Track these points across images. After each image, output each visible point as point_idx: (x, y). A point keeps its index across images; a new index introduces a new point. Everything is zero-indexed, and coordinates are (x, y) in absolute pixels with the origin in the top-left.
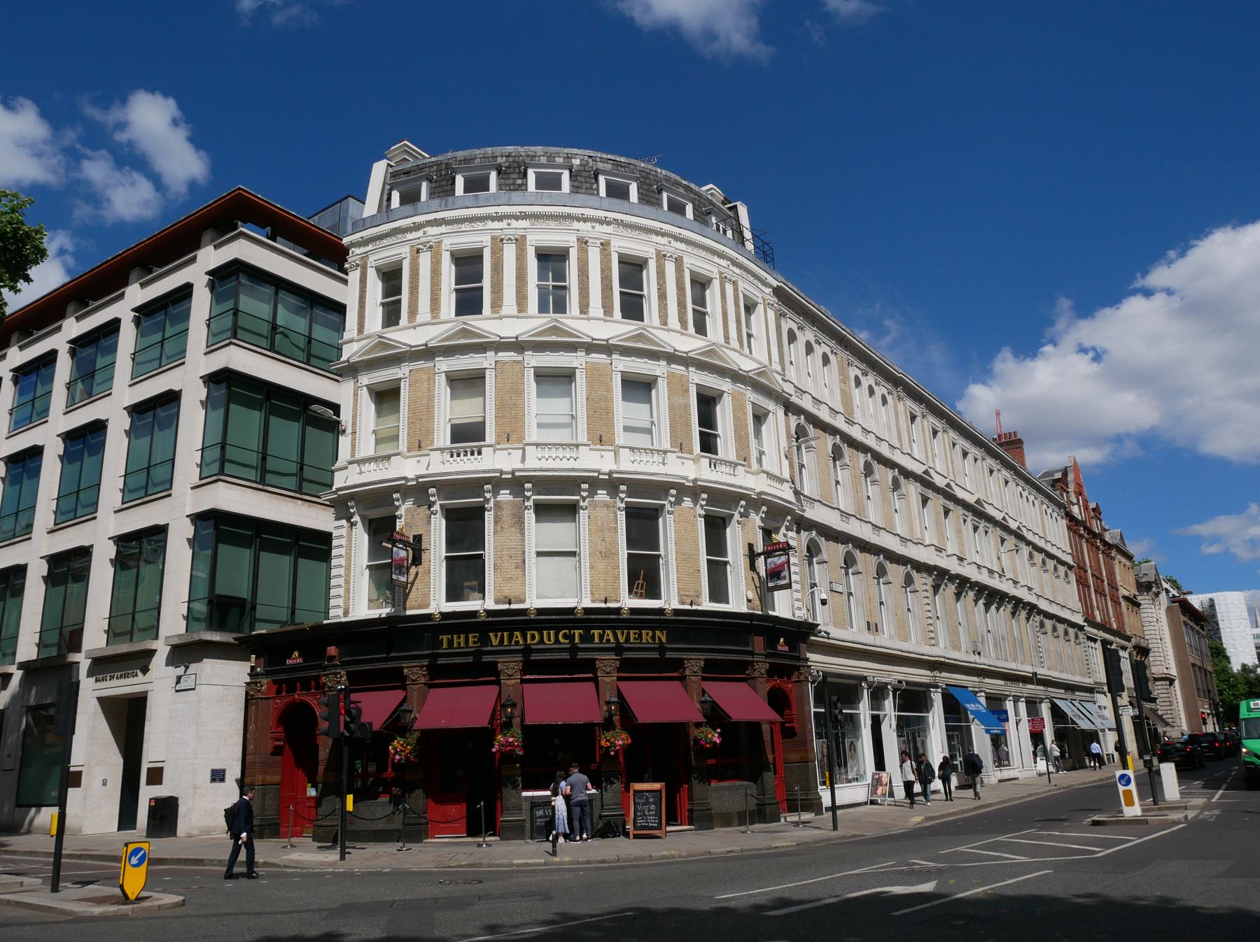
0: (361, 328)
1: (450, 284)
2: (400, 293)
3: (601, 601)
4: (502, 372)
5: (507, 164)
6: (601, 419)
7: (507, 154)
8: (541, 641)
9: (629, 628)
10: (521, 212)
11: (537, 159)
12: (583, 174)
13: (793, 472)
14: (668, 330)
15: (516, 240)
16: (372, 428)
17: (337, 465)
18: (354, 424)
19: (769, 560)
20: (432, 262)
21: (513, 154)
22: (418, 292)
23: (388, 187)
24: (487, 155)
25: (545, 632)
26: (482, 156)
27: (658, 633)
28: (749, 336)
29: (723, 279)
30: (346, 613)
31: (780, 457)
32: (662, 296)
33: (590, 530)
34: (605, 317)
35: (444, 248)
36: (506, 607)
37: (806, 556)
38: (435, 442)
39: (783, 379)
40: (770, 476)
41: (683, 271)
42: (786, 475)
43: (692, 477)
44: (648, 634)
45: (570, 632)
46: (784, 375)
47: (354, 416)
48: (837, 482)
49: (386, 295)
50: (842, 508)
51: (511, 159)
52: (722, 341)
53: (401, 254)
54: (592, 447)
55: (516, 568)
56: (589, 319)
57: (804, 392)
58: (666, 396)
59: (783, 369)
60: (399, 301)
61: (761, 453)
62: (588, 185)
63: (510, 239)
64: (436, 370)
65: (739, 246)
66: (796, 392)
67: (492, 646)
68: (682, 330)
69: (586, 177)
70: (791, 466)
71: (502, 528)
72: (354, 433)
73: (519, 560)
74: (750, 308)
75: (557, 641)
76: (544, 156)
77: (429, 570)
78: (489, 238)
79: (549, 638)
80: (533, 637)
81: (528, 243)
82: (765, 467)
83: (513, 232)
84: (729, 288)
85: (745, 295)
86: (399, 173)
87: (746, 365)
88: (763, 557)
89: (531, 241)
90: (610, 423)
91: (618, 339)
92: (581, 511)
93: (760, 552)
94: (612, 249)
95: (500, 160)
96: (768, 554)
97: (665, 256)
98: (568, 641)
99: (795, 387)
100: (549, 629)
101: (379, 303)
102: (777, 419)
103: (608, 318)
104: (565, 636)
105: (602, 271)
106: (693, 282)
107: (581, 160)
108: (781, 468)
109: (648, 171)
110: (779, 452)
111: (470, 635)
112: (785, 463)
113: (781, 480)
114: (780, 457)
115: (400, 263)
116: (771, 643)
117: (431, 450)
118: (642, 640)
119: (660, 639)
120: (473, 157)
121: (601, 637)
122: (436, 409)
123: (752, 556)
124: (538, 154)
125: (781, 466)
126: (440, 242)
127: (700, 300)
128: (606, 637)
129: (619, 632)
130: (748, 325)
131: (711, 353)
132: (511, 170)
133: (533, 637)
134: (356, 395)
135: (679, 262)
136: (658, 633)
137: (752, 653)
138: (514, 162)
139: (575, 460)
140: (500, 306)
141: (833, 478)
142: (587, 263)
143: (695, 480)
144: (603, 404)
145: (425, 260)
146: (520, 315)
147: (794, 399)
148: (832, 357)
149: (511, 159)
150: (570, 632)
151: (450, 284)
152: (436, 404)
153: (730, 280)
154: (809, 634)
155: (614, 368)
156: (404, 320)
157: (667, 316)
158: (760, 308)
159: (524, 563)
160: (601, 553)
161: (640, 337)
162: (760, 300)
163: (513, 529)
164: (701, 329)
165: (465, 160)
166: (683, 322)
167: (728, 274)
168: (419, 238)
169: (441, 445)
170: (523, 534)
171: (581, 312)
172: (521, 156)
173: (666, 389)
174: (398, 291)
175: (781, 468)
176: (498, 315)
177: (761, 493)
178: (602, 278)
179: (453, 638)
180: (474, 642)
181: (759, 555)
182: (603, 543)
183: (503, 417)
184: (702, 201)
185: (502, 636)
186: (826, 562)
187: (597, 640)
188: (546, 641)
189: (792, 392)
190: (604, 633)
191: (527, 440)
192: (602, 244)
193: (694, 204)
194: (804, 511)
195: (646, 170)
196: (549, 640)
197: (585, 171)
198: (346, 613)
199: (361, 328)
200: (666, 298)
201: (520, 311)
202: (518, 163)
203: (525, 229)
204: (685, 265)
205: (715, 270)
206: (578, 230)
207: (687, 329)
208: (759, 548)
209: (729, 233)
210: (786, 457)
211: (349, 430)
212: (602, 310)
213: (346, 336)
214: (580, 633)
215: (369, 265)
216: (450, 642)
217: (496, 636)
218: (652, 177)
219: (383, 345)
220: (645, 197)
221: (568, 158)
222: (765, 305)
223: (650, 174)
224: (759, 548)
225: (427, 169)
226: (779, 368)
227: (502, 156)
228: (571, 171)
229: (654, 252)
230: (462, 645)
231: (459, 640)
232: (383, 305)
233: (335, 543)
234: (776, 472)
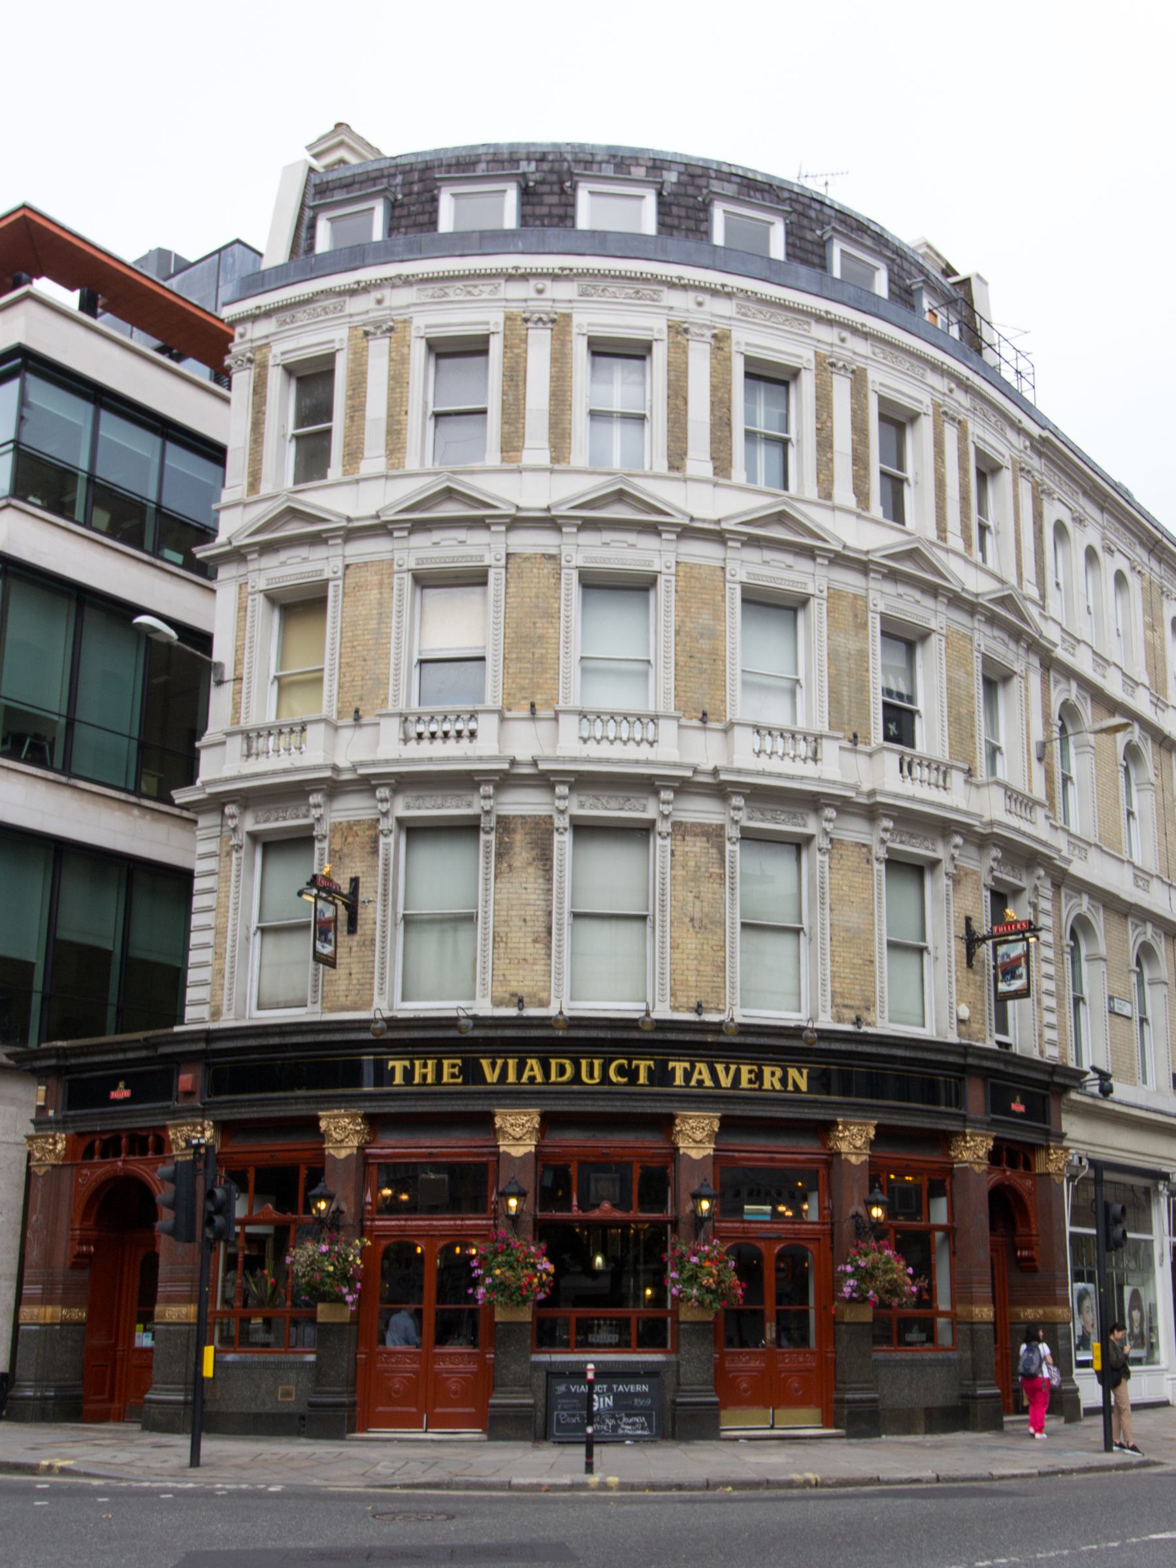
0: (254, 484)
1: (425, 403)
2: (330, 419)
3: (689, 1009)
4: (520, 576)
5: (538, 176)
6: (702, 672)
7: (538, 156)
8: (576, 1080)
9: (740, 1060)
10: (563, 269)
11: (595, 167)
12: (683, 201)
13: (1053, 790)
14: (834, 508)
15: (553, 321)
16: (273, 672)
17: (206, 739)
18: (238, 663)
19: (1002, 950)
20: (391, 360)
21: (550, 157)
22: (363, 417)
23: (308, 213)
24: (500, 157)
25: (584, 1062)
26: (490, 158)
28: (983, 528)
29: (942, 415)
30: (216, 1014)
31: (1029, 759)
32: (825, 443)
33: (673, 877)
34: (716, 479)
35: (414, 333)
36: (512, 1012)
37: (1068, 945)
38: (390, 702)
39: (1041, 614)
40: (1010, 793)
41: (866, 396)
42: (1039, 793)
43: (866, 787)
45: (630, 1064)
46: (1043, 608)
47: (239, 649)
48: (1130, 814)
49: (301, 421)
50: (1138, 861)
51: (546, 166)
52: (932, 535)
53: (332, 341)
54: (684, 722)
55: (535, 941)
56: (685, 480)
57: (1078, 641)
58: (825, 634)
59: (1043, 596)
60: (328, 432)
61: (994, 751)
62: (692, 224)
63: (540, 319)
64: (396, 568)
65: (974, 356)
66: (1063, 640)
67: (483, 1080)
68: (859, 511)
69: (687, 208)
70: (1049, 779)
71: (510, 866)
72: (238, 679)
73: (540, 927)
74: (987, 471)
75: (605, 1079)
76: (608, 162)
77: (373, 940)
78: (500, 318)
79: (591, 1072)
80: (562, 1071)
81: (575, 330)
82: (1002, 774)
83: (546, 306)
84: (951, 434)
85: (978, 450)
86: (331, 186)
87: (975, 583)
88: (990, 942)
89: (580, 326)
90: (717, 681)
91: (738, 520)
92: (659, 841)
93: (985, 933)
94: (734, 348)
95: (524, 167)
96: (999, 940)
97: (832, 365)
98: (625, 1080)
99: (1063, 630)
100: (591, 1055)
101: (289, 436)
102: (1026, 689)
103: (721, 481)
104: (621, 1071)
105: (714, 389)
106: (883, 418)
107: (680, 173)
108: (1030, 781)
109: (807, 201)
110: (1028, 750)
111: (446, 1063)
112: (1038, 772)
113: (1027, 803)
114: (1029, 759)
115: (330, 358)
116: (998, 1102)
117: (381, 716)
118: (762, 1084)
119: (795, 1084)
120: (473, 158)
121: (688, 1075)
122: (393, 640)
123: (972, 941)
124: (598, 158)
125: (1030, 777)
126: (407, 322)
127: (896, 454)
128: (696, 1076)
129: (720, 1068)
130: (982, 510)
131: (913, 555)
132: (545, 189)
133: (562, 1071)
134: (242, 609)
135: (858, 379)
136: (793, 1073)
137: (964, 1119)
138: (551, 171)
139: (651, 744)
140: (518, 449)
141: (1123, 807)
142: (685, 373)
143: (872, 793)
144: (705, 644)
145: (378, 356)
146: (557, 467)
147: (1060, 653)
148: (1131, 578)
149: (546, 166)
150: (630, 1064)
151: (425, 403)
152: (394, 630)
153: (953, 419)
154: (1066, 1089)
155: (728, 577)
156: (335, 472)
157: (831, 482)
158: (1006, 476)
159: (550, 933)
160: (692, 920)
161: (781, 518)
162: (1006, 462)
163: (531, 870)
164: (896, 512)
165: (458, 164)
166: (862, 496)
167: (950, 405)
168: (367, 312)
169: (402, 707)
170: (549, 880)
171: (672, 467)
172: (565, 160)
173: (825, 620)
174: (326, 413)
175: (1030, 781)
176: (513, 466)
177: (992, 823)
178: (712, 403)
179: (413, 1065)
180: (453, 1076)
181: (984, 939)
182: (697, 903)
183: (519, 659)
184: (906, 265)
186: (1104, 960)
188: (584, 1077)
189: (1058, 640)
190: (693, 1067)
191: (561, 705)
192: (715, 336)
193: (890, 271)
194: (1069, 862)
195: (801, 199)
196: (591, 1076)
197: (687, 195)
198: (216, 1014)
199: (254, 484)
200: (831, 447)
201: (555, 460)
202: (559, 173)
203: (570, 301)
204: (870, 386)
205: (927, 400)
206: (671, 308)
207: (867, 508)
208: (983, 925)
209: (954, 332)
210: (1040, 759)
211: (228, 674)
213: (227, 496)
214: (649, 1068)
215: (271, 362)
216: (408, 1074)
217: (493, 1065)
218: (813, 214)
219: (293, 514)
220: (798, 253)
221: (654, 167)
222: (1014, 472)
223: (810, 207)
224: (983, 925)
225: (385, 180)
226: (1034, 592)
227: (529, 160)
228: (660, 194)
229: (812, 356)
230: (429, 1080)
231: (425, 1070)
232: (298, 438)
233: (198, 884)
234: (1019, 785)
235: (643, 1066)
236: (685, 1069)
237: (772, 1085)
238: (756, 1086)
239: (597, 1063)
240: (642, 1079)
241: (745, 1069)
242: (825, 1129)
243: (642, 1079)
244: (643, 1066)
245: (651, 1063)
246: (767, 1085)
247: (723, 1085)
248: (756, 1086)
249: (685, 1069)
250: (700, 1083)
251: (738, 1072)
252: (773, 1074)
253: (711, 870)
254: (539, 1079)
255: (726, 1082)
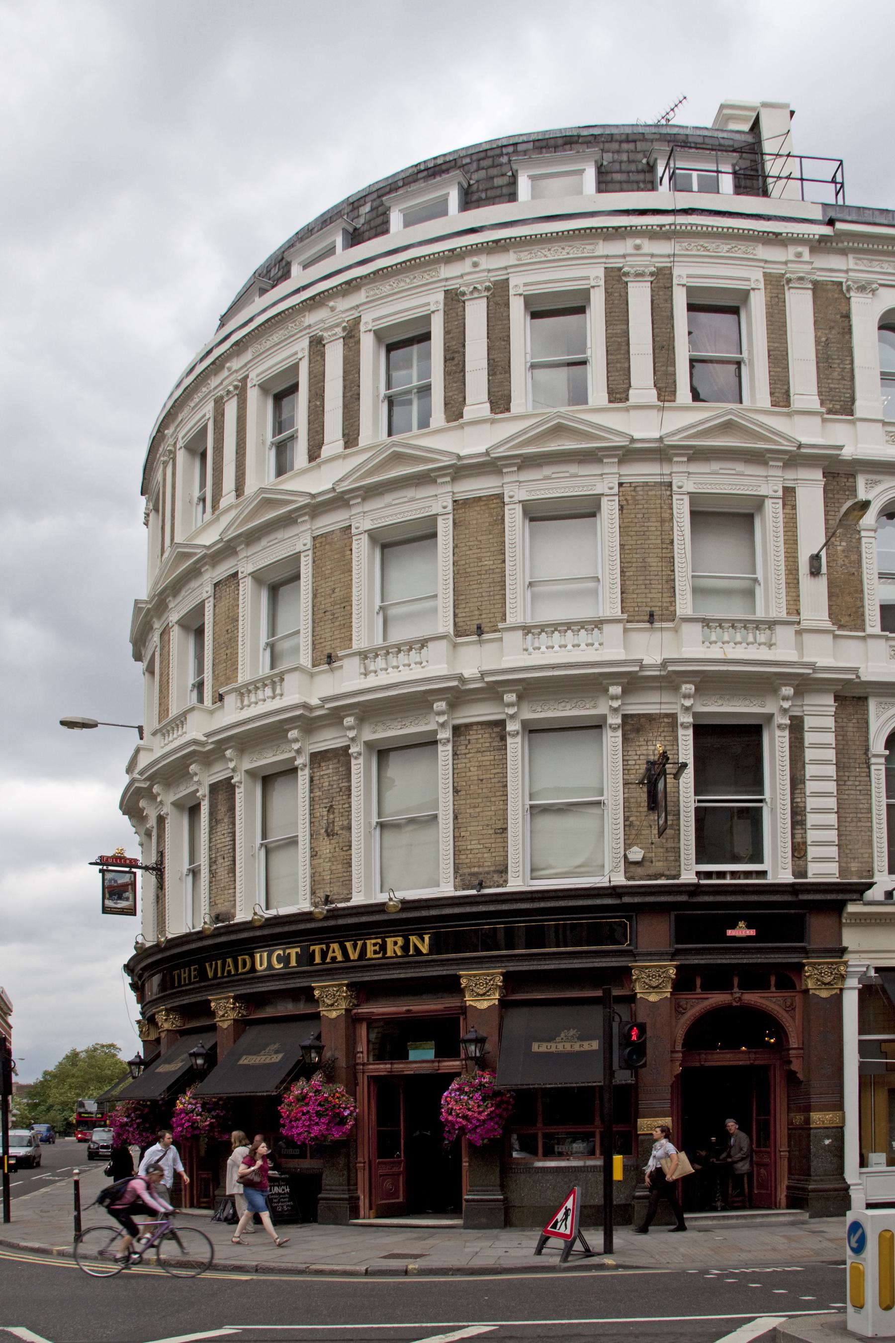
8: (253, 969)
9: (360, 937)
27: (413, 939)
44: (396, 943)
45: (284, 953)
67: (208, 979)
75: (270, 966)
111: (192, 968)
118: (385, 952)
119: (415, 946)
121: (324, 954)
128: (330, 954)
129: (348, 945)
136: (413, 939)
185: (216, 964)
187: (318, 960)
188: (258, 967)
190: (328, 948)
212: (654, 392)
235: (293, 952)
236: (322, 950)
237: (395, 952)
238: (380, 955)
239: (265, 954)
240: (293, 963)
241: (389, 941)
242: (452, 986)
243: (293, 963)
244: (293, 952)
245: (298, 950)
246: (389, 953)
247: (352, 958)
248: (380, 955)
249: (322, 950)
250: (334, 959)
251: (364, 946)
252: (396, 943)
253: (341, 785)
254: (340, 958)
255: (354, 955)
